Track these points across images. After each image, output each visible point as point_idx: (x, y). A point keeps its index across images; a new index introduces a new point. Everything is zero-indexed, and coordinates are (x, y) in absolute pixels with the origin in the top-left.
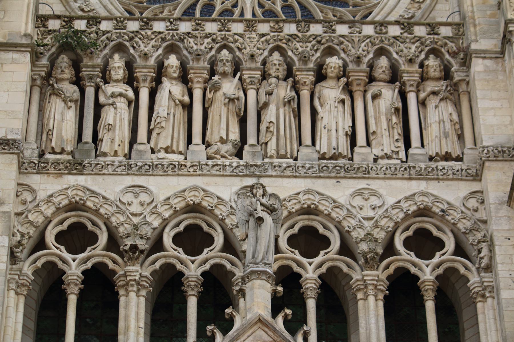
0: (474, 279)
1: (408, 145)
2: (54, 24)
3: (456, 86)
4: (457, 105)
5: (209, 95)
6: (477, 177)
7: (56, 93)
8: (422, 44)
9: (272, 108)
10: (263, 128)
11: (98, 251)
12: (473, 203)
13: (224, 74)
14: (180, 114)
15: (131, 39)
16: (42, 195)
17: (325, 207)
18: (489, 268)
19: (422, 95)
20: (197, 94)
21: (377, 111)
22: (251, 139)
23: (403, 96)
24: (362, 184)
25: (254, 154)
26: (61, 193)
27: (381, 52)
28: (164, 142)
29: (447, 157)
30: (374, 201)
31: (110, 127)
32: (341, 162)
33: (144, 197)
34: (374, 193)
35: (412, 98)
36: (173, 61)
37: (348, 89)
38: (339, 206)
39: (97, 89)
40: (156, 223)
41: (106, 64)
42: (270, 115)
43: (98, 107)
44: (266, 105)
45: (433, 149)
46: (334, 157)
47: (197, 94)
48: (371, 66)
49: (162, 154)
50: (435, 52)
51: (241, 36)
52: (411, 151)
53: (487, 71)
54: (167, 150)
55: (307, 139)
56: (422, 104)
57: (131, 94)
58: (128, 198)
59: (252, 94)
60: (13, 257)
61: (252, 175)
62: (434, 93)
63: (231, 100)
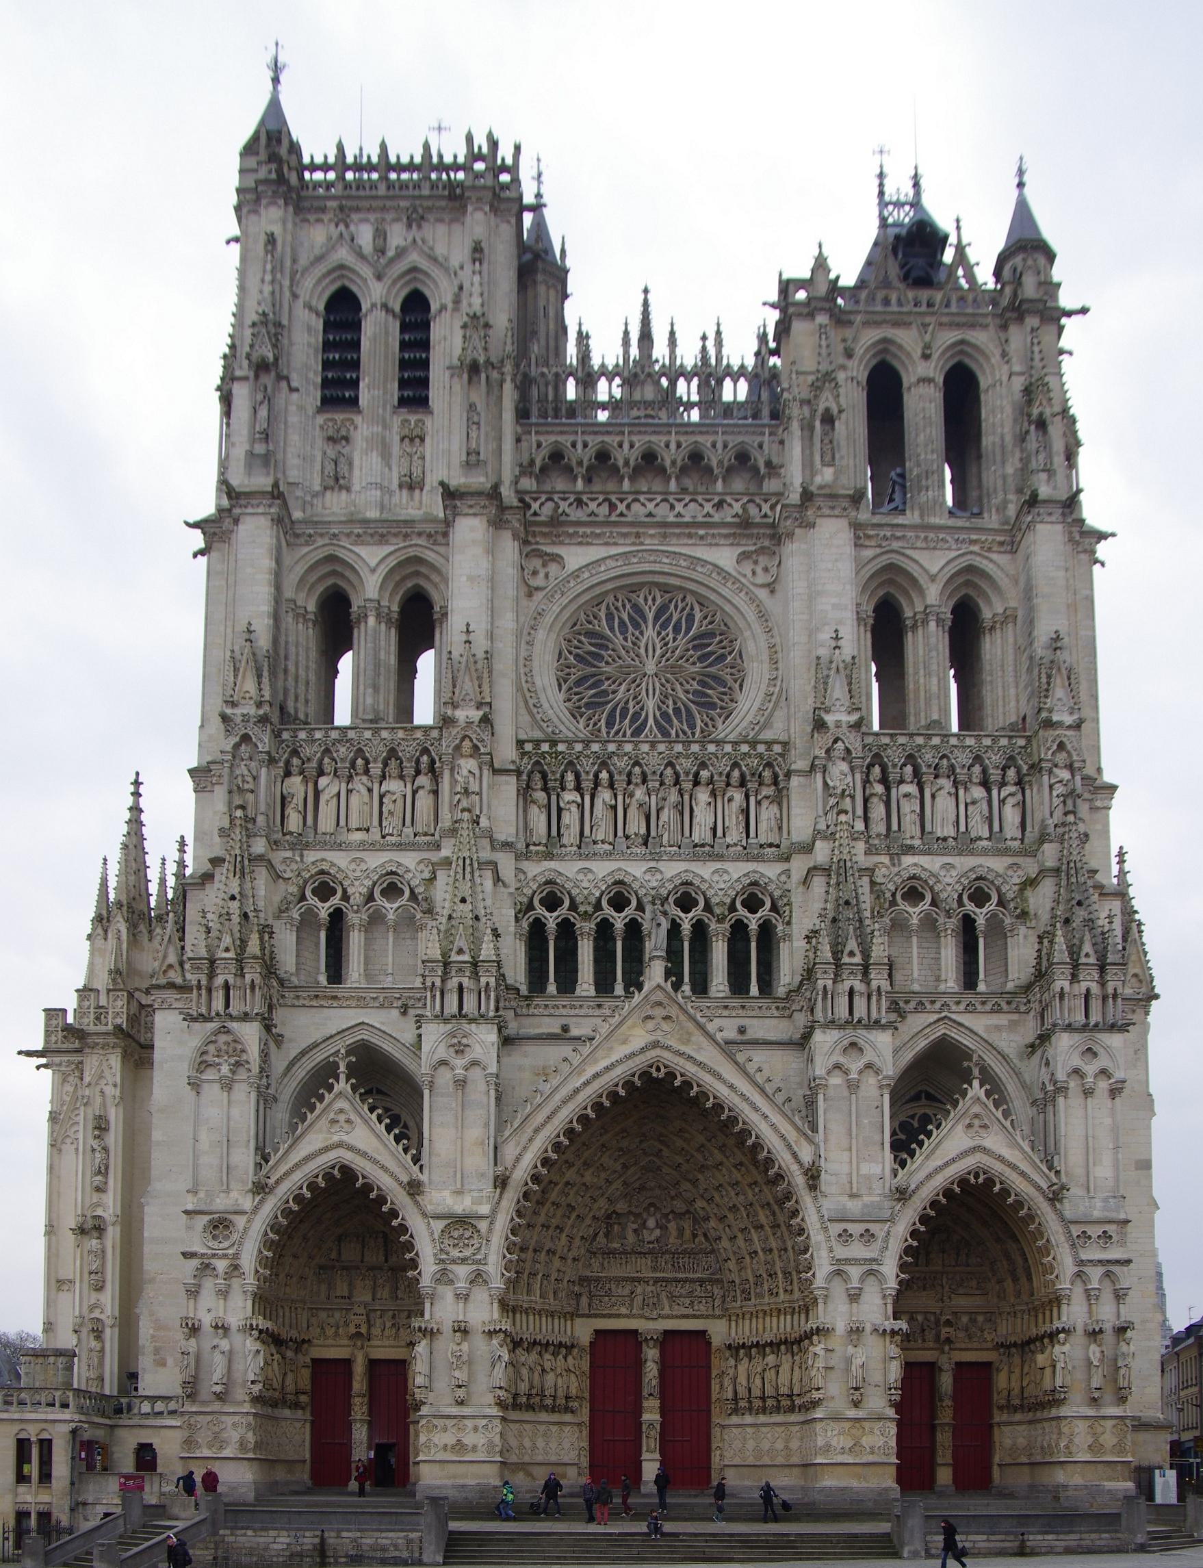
0: (780, 928)
1: (748, 836)
2: (528, 747)
3: (780, 791)
4: (780, 804)
5: (627, 801)
6: (788, 859)
7: (533, 802)
8: (762, 758)
9: (666, 810)
10: (661, 823)
11: (564, 911)
12: (783, 878)
13: (637, 784)
14: (610, 814)
15: (578, 758)
16: (530, 875)
17: (697, 882)
18: (789, 923)
19: (759, 797)
20: (620, 798)
21: (730, 811)
22: (653, 833)
23: (747, 797)
24: (718, 865)
25: (654, 844)
26: (540, 874)
27: (736, 765)
28: (600, 837)
29: (771, 845)
30: (726, 877)
31: (568, 827)
32: (707, 849)
33: (590, 876)
34: (726, 872)
35: (752, 799)
36: (604, 775)
37: (713, 794)
38: (705, 881)
39: (558, 795)
40: (597, 895)
41: (562, 776)
42: (664, 816)
43: (560, 810)
44: (662, 808)
45: (763, 839)
46: (703, 846)
47: (620, 798)
48: (728, 776)
49: (600, 846)
50: (769, 765)
51: (648, 754)
52: (750, 841)
53: (800, 786)
54: (603, 842)
55: (687, 833)
56: (758, 803)
57: (579, 800)
58: (580, 877)
59: (653, 798)
60: (517, 920)
61: (653, 860)
62: (766, 797)
63: (641, 805)
